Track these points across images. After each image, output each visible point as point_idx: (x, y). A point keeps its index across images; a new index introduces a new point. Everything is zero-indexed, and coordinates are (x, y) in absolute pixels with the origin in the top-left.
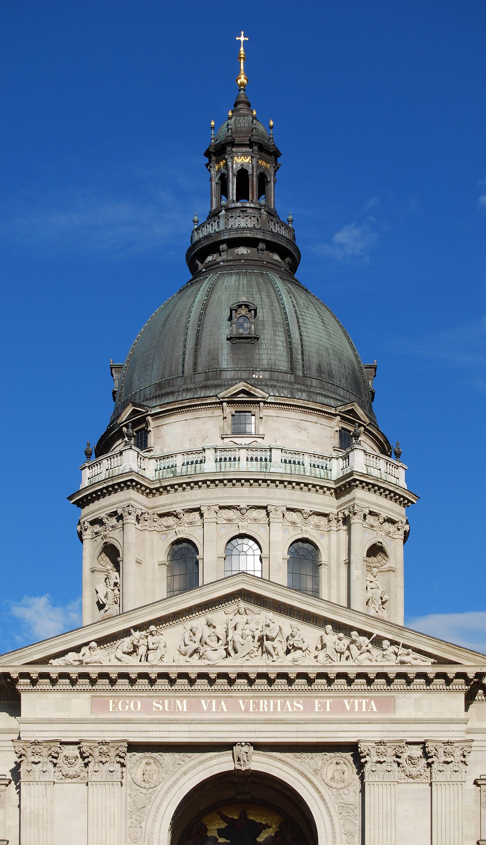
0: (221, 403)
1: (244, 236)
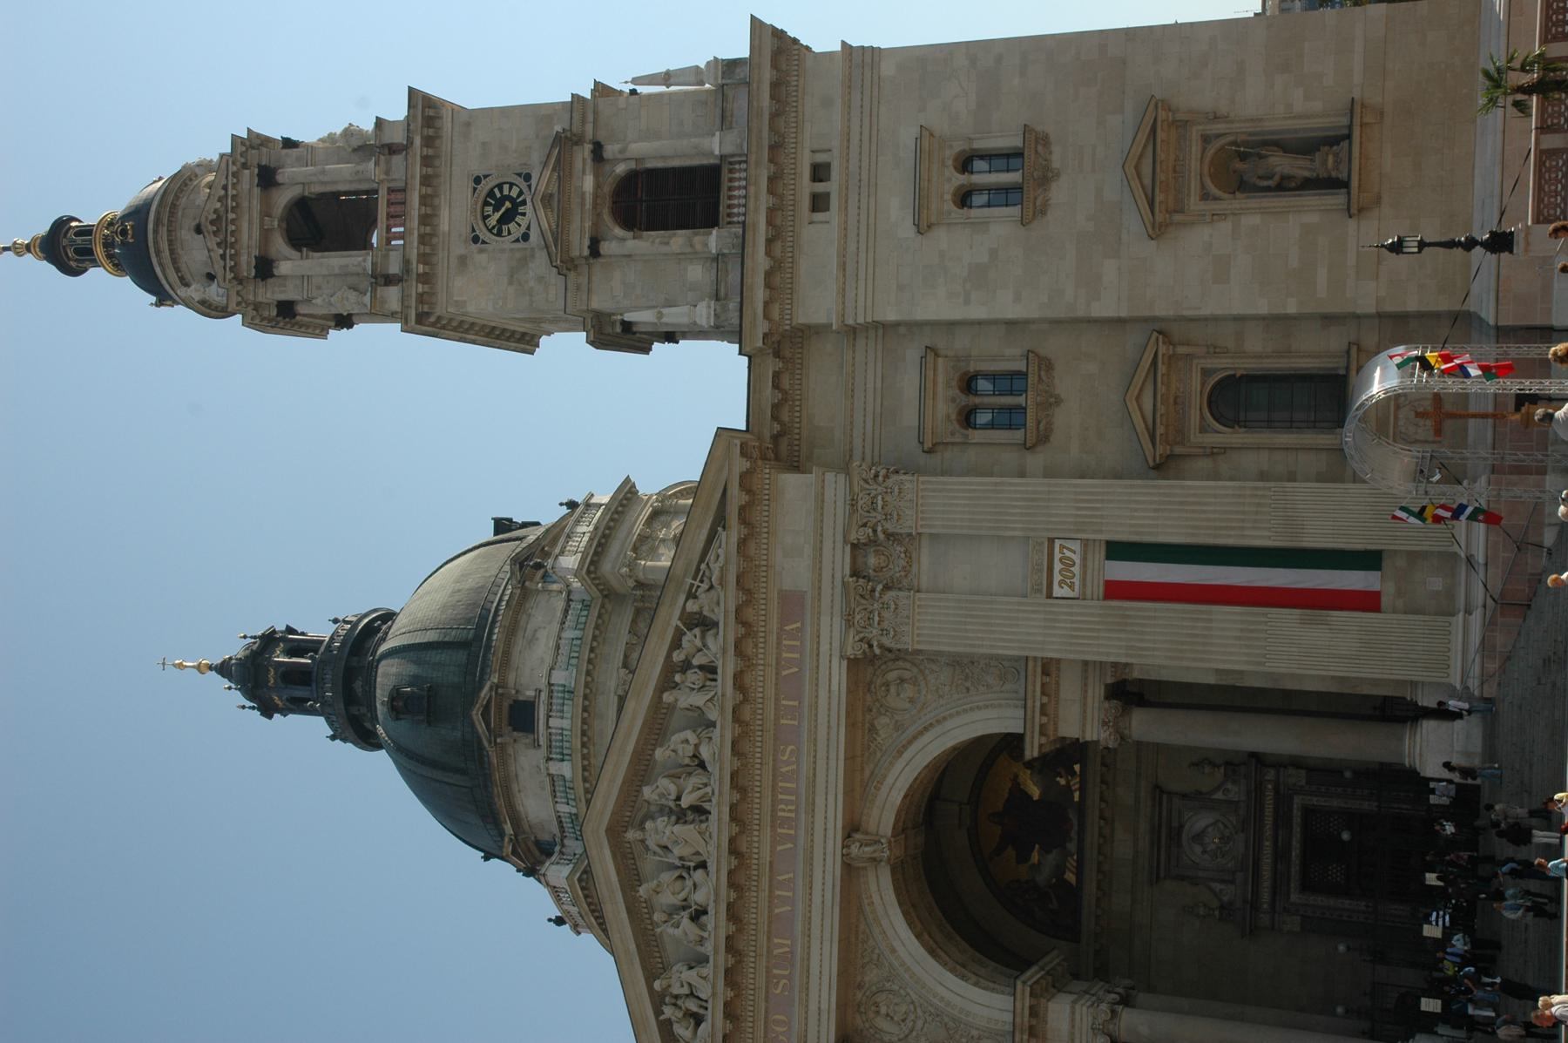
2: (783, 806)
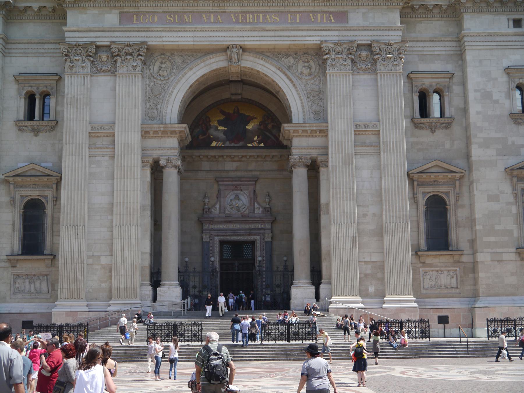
2: (251, 16)
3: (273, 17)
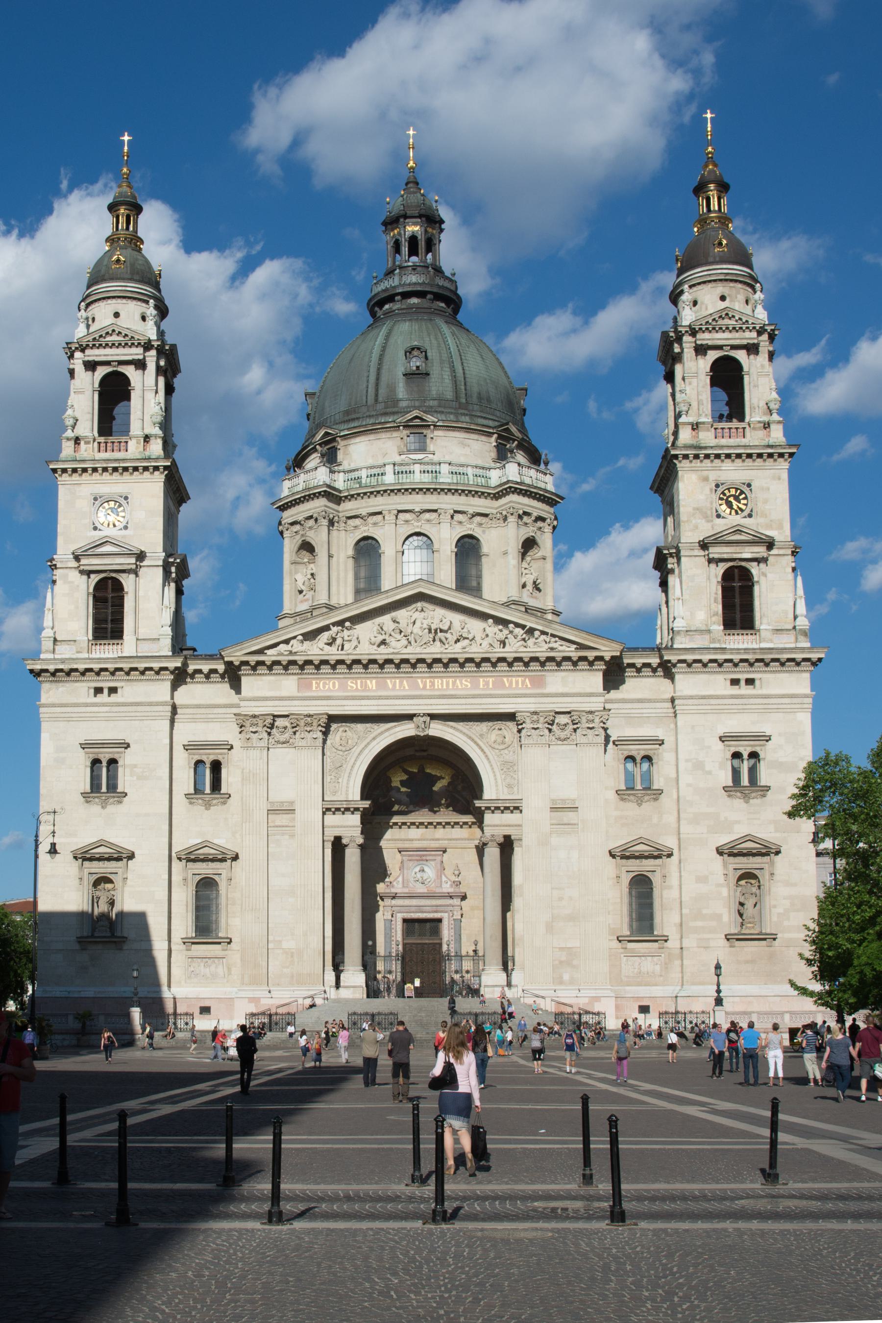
0: (399, 427)
1: (415, 289)
3: (464, 682)
